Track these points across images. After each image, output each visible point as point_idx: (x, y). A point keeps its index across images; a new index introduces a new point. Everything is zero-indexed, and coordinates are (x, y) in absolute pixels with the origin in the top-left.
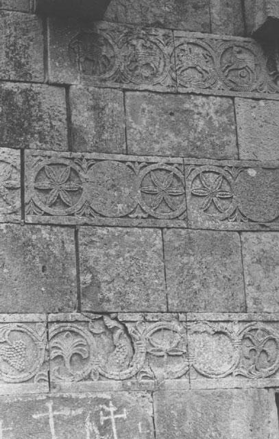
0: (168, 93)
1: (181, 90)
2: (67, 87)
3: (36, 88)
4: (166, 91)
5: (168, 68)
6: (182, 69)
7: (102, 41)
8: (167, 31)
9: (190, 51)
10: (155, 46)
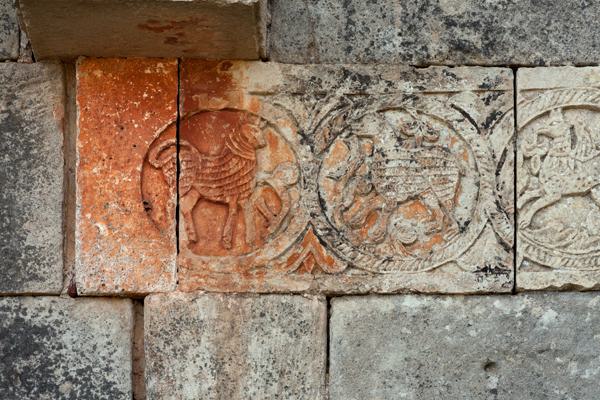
0: (480, 294)
1: (525, 280)
2: (138, 300)
3: (36, 311)
4: (474, 288)
5: (489, 203)
6: (541, 203)
7: (258, 135)
8: (493, 73)
9: (574, 141)
10: (445, 132)
